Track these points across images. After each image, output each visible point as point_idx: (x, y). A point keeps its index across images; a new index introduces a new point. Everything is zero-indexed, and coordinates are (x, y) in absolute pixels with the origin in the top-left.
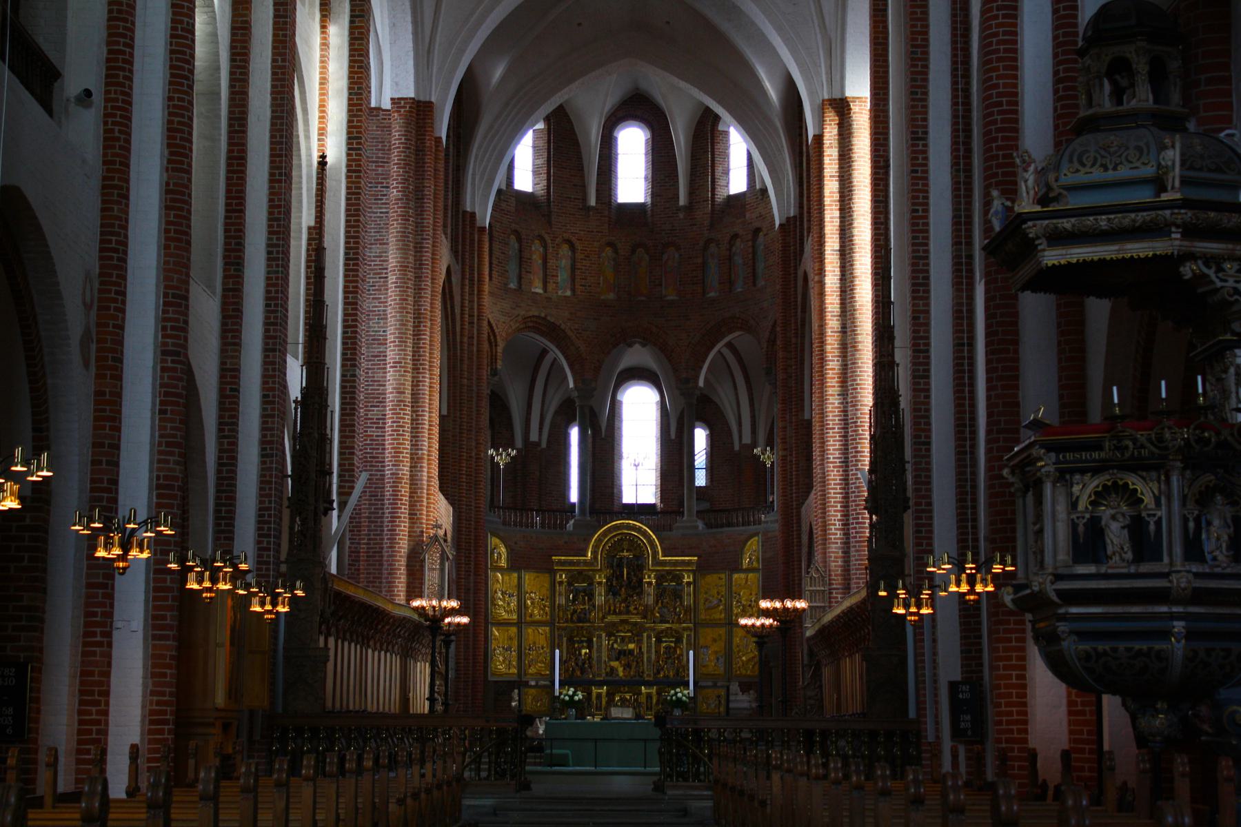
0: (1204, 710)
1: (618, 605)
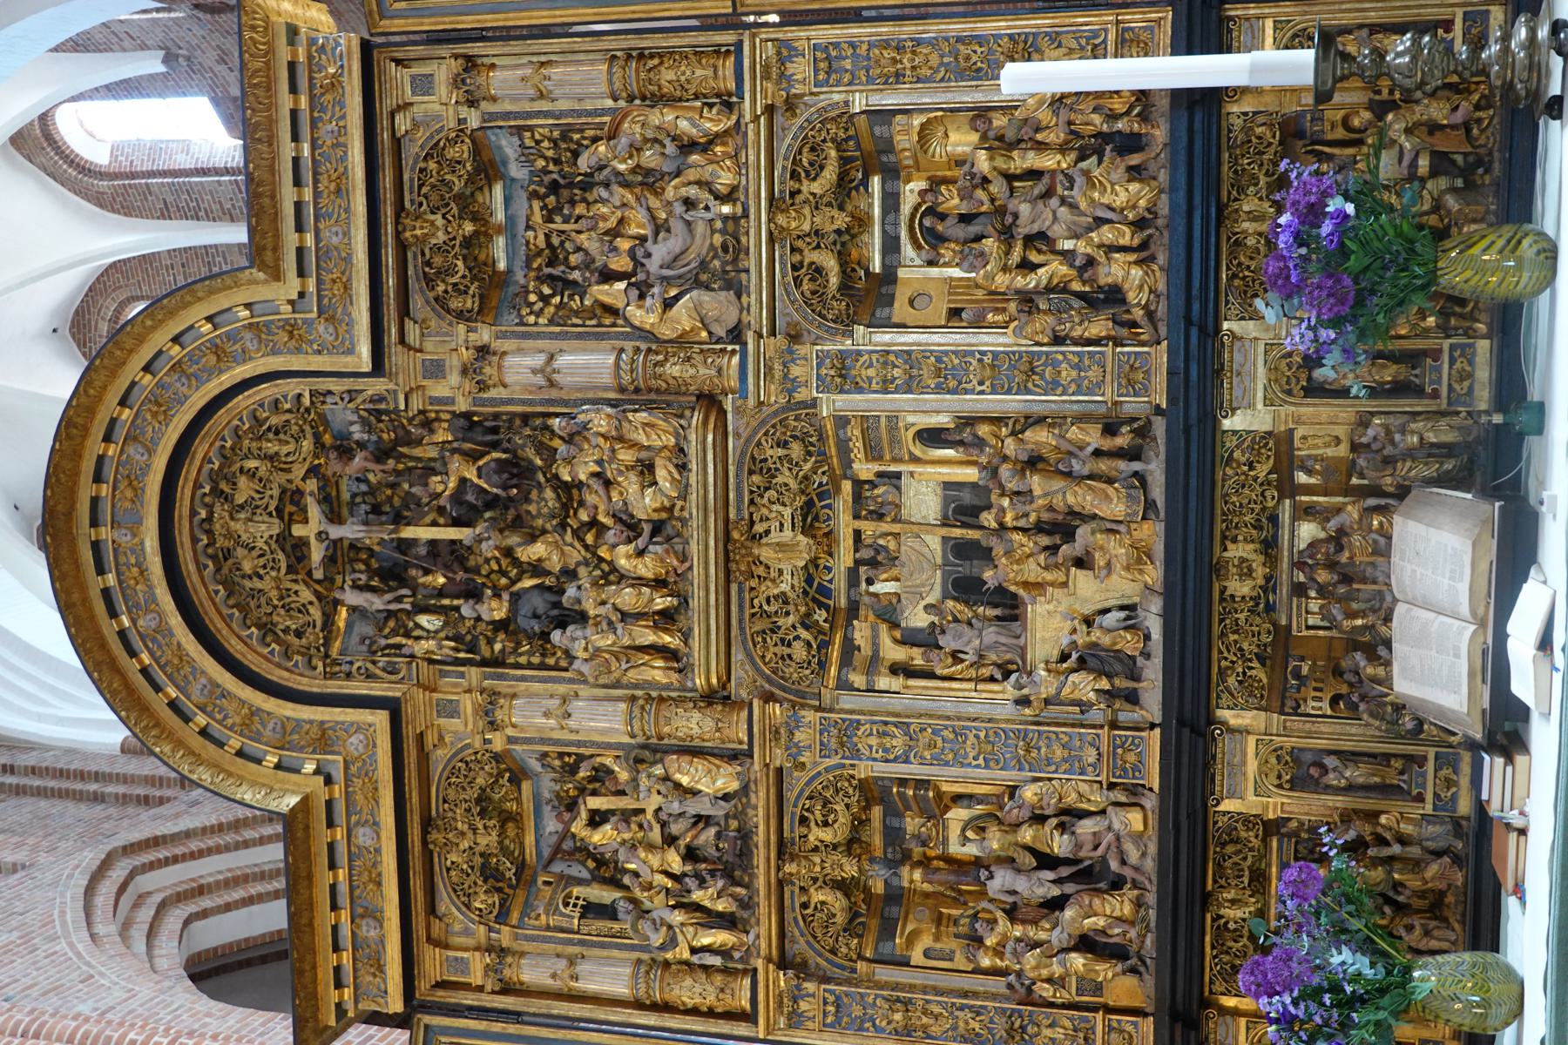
1: (627, 598)
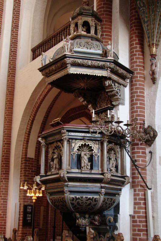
0: (97, 218)
